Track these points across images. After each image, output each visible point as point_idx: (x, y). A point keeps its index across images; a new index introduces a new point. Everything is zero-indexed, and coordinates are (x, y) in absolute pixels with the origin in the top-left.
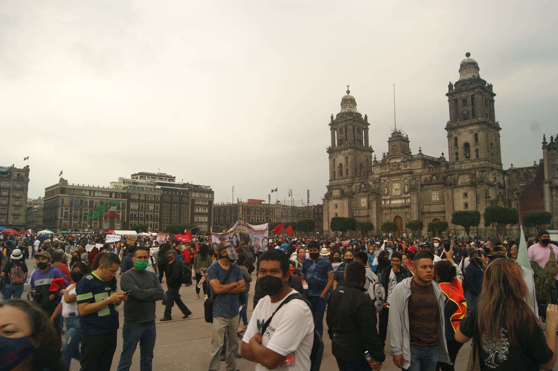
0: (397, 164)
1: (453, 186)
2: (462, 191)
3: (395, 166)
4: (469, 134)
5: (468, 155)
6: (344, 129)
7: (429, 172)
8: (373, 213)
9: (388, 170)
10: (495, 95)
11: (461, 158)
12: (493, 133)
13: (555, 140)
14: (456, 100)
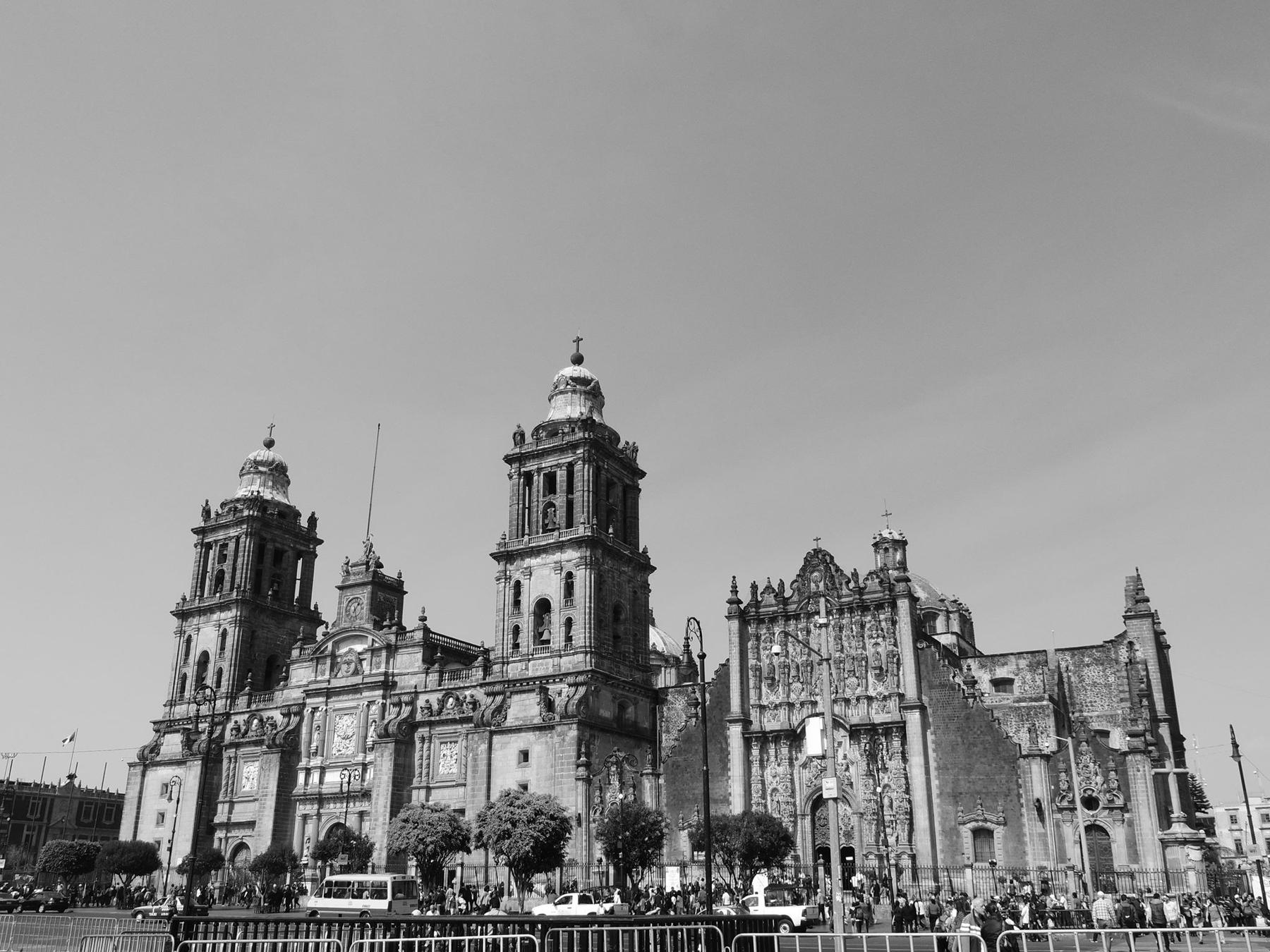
0: (353, 658)
1: (493, 728)
2: (517, 742)
3: (348, 663)
4: (553, 574)
5: (545, 637)
6: (232, 545)
7: (440, 685)
8: (266, 813)
9: (327, 676)
10: (642, 474)
11: (526, 643)
12: (624, 578)
13: (761, 593)
14: (528, 477)
